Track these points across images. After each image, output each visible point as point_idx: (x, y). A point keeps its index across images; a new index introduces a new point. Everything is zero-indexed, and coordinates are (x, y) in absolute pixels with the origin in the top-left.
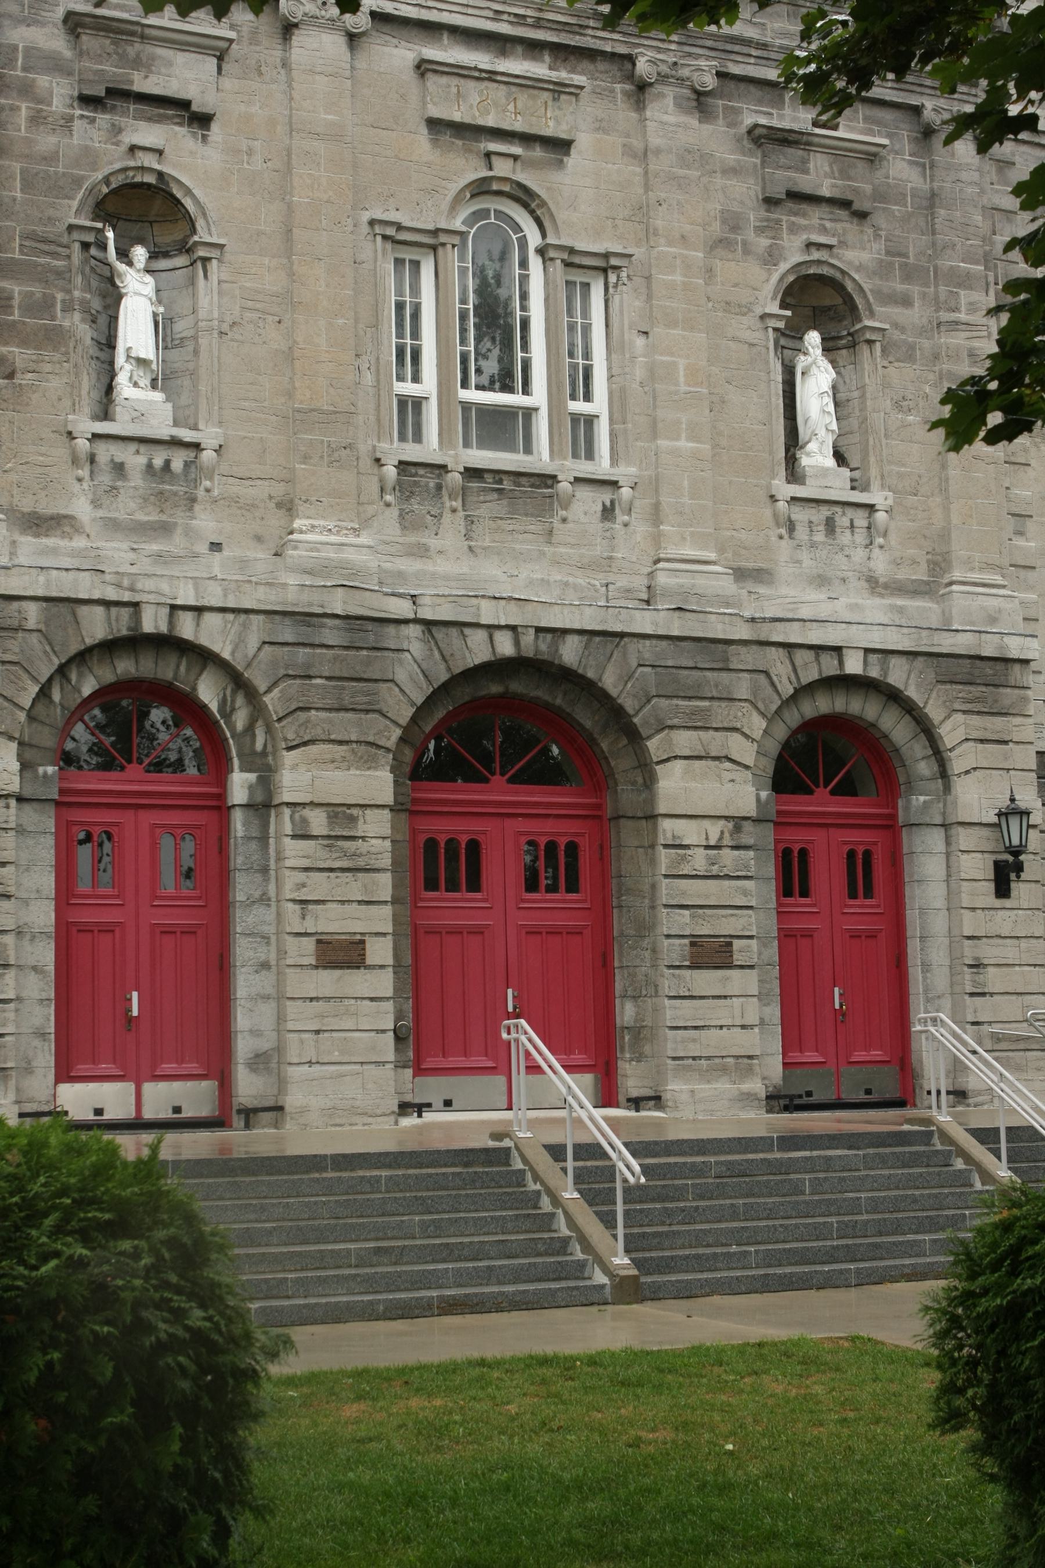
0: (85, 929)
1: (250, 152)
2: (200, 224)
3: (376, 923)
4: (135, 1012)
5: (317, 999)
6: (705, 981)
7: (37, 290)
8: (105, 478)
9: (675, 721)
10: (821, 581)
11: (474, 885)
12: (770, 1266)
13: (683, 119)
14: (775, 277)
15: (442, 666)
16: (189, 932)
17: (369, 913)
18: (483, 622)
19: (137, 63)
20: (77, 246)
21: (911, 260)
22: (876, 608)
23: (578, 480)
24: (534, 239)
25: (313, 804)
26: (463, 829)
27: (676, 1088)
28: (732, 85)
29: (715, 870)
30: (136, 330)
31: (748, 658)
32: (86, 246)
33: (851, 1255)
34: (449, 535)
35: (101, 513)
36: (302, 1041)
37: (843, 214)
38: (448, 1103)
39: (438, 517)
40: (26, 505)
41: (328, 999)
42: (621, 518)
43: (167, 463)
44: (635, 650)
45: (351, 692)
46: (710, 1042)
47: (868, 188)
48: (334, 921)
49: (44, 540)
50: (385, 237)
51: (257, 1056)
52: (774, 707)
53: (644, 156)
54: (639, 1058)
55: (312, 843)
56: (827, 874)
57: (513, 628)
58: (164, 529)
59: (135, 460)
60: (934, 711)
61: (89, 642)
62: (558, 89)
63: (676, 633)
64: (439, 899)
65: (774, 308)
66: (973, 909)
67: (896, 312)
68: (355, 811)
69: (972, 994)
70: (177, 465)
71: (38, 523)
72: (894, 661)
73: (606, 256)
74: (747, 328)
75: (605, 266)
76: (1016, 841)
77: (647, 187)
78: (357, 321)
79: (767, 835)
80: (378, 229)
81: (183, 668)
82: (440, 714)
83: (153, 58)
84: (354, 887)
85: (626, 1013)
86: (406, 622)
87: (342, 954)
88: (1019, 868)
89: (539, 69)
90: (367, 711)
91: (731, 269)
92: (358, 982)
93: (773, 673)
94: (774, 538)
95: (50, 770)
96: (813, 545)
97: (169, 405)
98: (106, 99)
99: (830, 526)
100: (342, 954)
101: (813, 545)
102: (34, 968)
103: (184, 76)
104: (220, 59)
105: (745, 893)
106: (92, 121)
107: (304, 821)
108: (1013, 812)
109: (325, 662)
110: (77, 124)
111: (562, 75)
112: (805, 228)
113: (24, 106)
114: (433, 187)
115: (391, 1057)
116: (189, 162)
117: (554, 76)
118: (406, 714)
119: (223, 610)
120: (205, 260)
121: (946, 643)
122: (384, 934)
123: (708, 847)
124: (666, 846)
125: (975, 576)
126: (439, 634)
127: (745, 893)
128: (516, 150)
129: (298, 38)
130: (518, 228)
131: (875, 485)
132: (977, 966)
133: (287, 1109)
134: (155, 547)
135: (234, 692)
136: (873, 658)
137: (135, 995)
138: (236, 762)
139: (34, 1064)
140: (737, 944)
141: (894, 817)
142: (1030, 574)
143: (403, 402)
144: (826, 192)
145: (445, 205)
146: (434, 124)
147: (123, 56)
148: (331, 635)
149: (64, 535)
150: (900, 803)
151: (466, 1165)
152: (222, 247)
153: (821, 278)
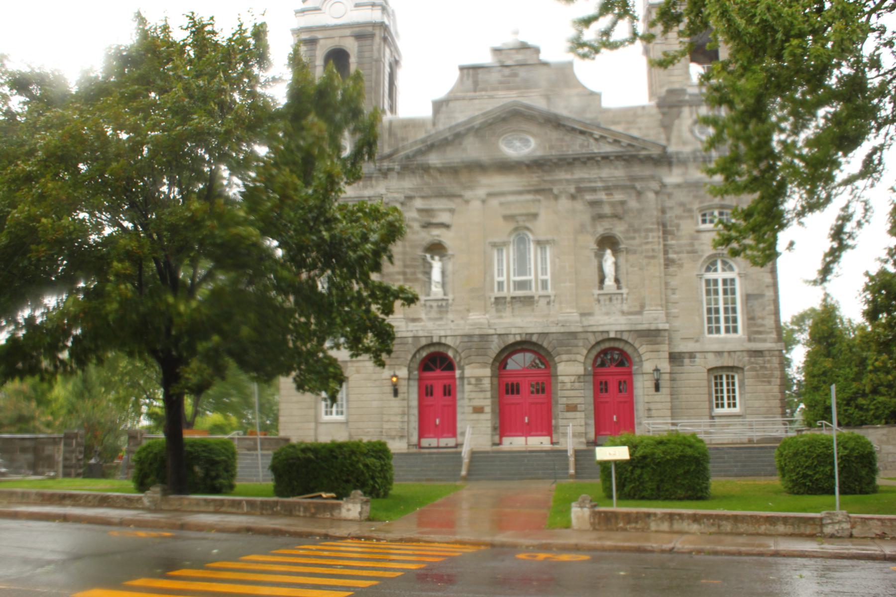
6: (570, 415)
7: (412, 270)
10: (608, 314)
11: (518, 392)
17: (486, 401)
19: (433, 217)
22: (623, 320)
23: (540, 297)
27: (562, 440)
30: (436, 275)
31: (582, 336)
40: (411, 316)
42: (552, 304)
44: (551, 337)
48: (477, 403)
54: (556, 433)
57: (520, 334)
58: (441, 319)
59: (434, 304)
60: (637, 345)
64: (507, 396)
67: (632, 242)
71: (414, 320)
75: (547, 242)
79: (590, 379)
84: (482, 395)
87: (478, 410)
96: (605, 305)
98: (427, 225)
99: (611, 300)
100: (478, 410)
102: (414, 415)
103: (444, 218)
104: (452, 211)
108: (657, 370)
118: (494, 355)
121: (639, 327)
132: (649, 410)
148: (476, 339)
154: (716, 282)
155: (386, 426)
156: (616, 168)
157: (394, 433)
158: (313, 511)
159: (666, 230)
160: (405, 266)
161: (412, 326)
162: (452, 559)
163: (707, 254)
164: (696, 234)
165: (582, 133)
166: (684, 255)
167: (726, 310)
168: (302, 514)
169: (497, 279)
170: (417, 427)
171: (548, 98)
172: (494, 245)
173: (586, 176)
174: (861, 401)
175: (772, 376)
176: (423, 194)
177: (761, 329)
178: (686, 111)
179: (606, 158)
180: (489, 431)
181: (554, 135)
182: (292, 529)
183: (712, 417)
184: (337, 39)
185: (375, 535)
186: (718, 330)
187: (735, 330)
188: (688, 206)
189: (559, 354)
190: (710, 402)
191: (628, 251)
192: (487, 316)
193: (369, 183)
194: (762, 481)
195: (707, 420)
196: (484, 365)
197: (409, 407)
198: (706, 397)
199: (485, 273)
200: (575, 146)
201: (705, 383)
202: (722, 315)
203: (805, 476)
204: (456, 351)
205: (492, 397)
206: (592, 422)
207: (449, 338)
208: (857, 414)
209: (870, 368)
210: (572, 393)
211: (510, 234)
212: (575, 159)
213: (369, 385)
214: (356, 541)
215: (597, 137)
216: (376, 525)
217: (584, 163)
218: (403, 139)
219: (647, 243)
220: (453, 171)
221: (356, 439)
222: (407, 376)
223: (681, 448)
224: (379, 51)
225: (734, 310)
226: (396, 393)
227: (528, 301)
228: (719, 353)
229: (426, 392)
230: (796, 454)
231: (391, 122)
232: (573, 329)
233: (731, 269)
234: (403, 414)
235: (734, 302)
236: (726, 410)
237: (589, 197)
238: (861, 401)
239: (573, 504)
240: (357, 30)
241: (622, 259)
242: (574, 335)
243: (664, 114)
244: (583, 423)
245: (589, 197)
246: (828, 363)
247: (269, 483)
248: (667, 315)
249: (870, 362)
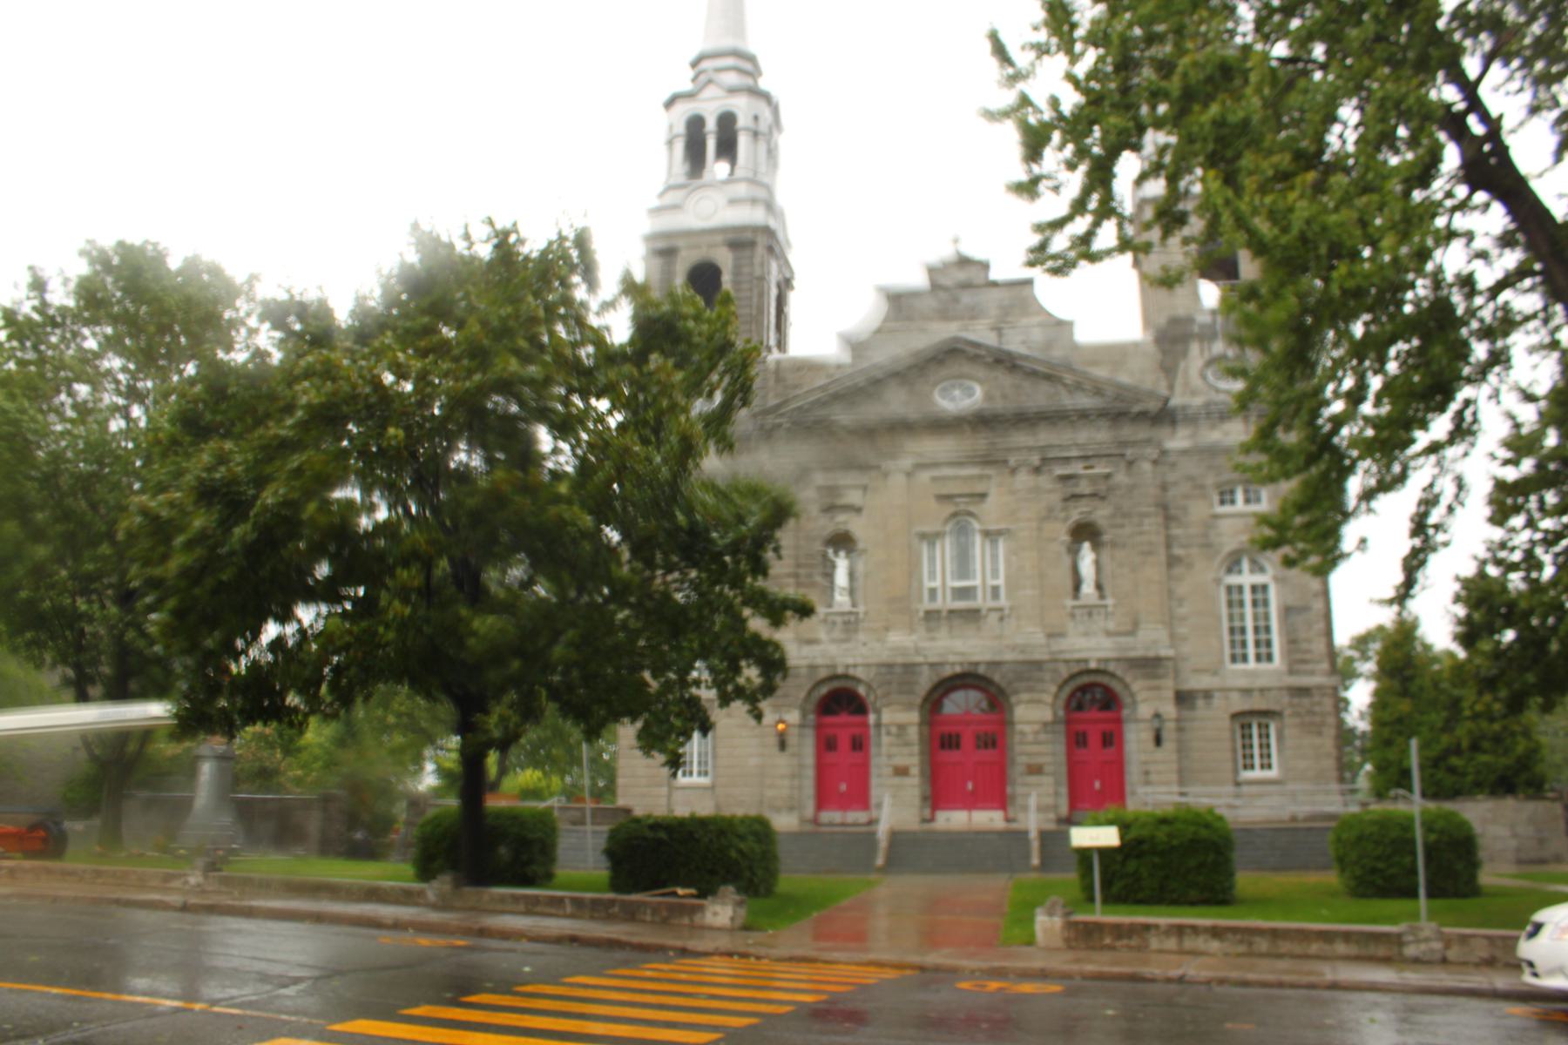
10: (1086, 634)
17: (912, 758)
23: (990, 610)
27: (1021, 816)
30: (841, 578)
34: (943, 632)
48: (900, 761)
56: (1094, 739)
59: (839, 619)
60: (1128, 679)
62: (981, 477)
71: (812, 642)
75: (1000, 533)
79: (1062, 728)
84: (906, 750)
87: (902, 772)
92: (907, 781)
98: (830, 509)
100: (902, 772)
103: (854, 497)
104: (865, 488)
108: (1157, 716)
121: (1132, 654)
132: (1147, 773)
154: (1240, 588)
155: (769, 793)
158: (665, 914)
159: (1168, 515)
160: (798, 566)
161: (807, 650)
162: (865, 988)
163: (1227, 549)
165: (1048, 377)
166: (1194, 551)
167: (1256, 630)
168: (648, 918)
169: (928, 584)
171: (998, 330)
172: (923, 536)
173: (1057, 442)
174: (1455, 761)
175: (1323, 724)
177: (1308, 657)
178: (1195, 348)
179: (1084, 415)
180: (917, 801)
181: (1006, 380)
182: (635, 940)
183: (1238, 784)
185: (752, 950)
186: (1245, 658)
187: (1269, 658)
189: (1016, 692)
190: (1235, 761)
191: (1114, 545)
192: (914, 637)
194: (1313, 878)
195: (1230, 789)
196: (908, 707)
197: (801, 766)
198: (1229, 755)
199: (910, 579)
200: (1038, 397)
201: (1227, 735)
202: (1250, 637)
203: (1374, 871)
204: (869, 687)
205: (922, 753)
206: (1064, 790)
208: (1449, 780)
209: (1467, 713)
210: (1035, 748)
211: (946, 521)
214: (727, 959)
216: (754, 937)
218: (796, 387)
219: (1141, 533)
221: (727, 812)
223: (1192, 829)
224: (762, 264)
225: (1268, 629)
226: (783, 745)
227: (973, 615)
228: (1247, 692)
229: (826, 745)
230: (1360, 838)
231: (778, 363)
232: (1037, 656)
233: (1262, 570)
234: (793, 776)
235: (1267, 617)
236: (1257, 774)
238: (1455, 761)
239: (1038, 910)
240: (731, 236)
241: (1106, 555)
242: (1038, 665)
243: (1164, 352)
244: (1051, 790)
245: (1060, 470)
246: (1405, 706)
247: (603, 873)
248: (1172, 636)
249: (1465, 704)
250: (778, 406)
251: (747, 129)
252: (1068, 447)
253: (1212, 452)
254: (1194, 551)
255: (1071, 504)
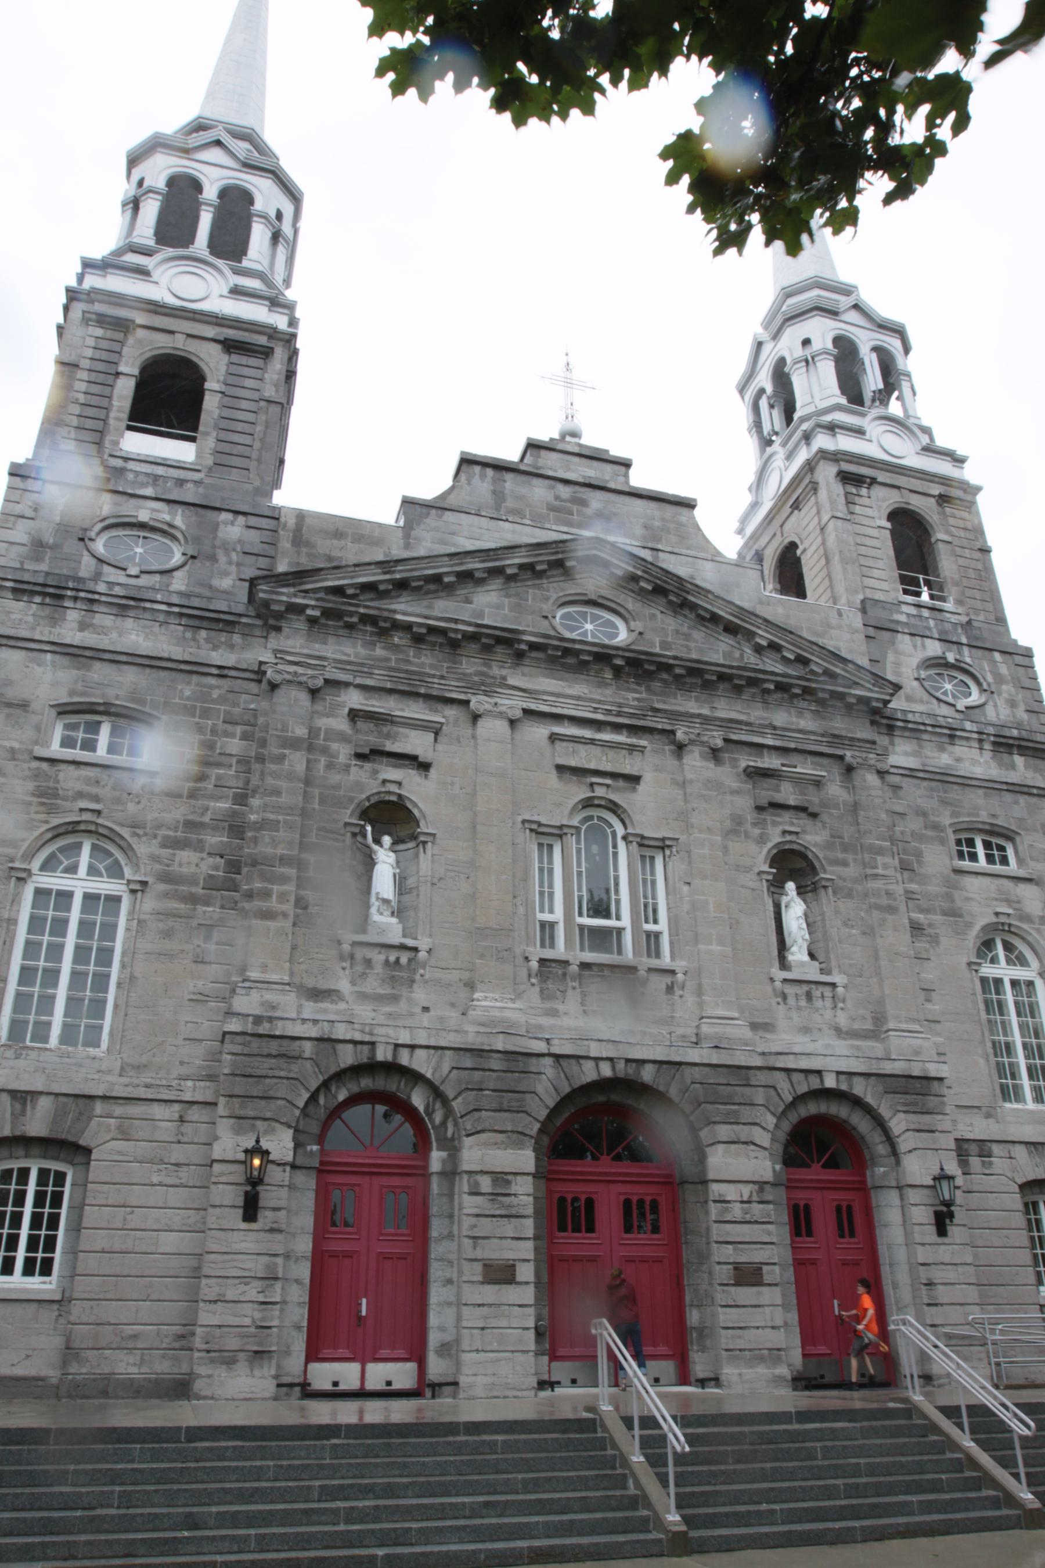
0: (334, 1255)
1: (453, 784)
2: (422, 823)
3: (524, 1254)
4: (364, 1313)
5: (482, 1305)
6: (745, 1294)
8: (359, 968)
9: (717, 1119)
10: (806, 1030)
11: (591, 1229)
12: (792, 1522)
13: (705, 764)
14: (765, 851)
15: (566, 1084)
16: (402, 1258)
18: (592, 1055)
19: (388, 736)
20: (349, 835)
21: (846, 840)
22: (842, 1047)
23: (651, 970)
24: (620, 831)
25: (483, 1172)
26: (583, 1190)
27: (729, 1372)
28: (732, 746)
29: (748, 1217)
31: (762, 1078)
32: (354, 835)
33: (856, 1513)
34: (571, 1004)
35: (356, 989)
36: (472, 1335)
37: (803, 815)
38: (574, 1381)
39: (564, 992)
40: (310, 983)
41: (490, 1305)
43: (398, 959)
44: (689, 1073)
45: (508, 1099)
46: (749, 1339)
47: (816, 800)
49: (320, 1005)
50: (531, 830)
51: (443, 1345)
52: (781, 1109)
53: (683, 784)
54: (703, 1349)
55: (481, 1198)
56: (824, 1221)
57: (611, 1059)
58: (394, 998)
59: (378, 957)
60: (885, 1112)
61: (342, 1066)
63: (715, 1062)
65: (766, 868)
66: (923, 1244)
67: (840, 869)
68: (509, 1177)
69: (929, 1305)
70: (404, 960)
71: (317, 994)
72: (856, 1080)
73: (663, 839)
74: (749, 880)
75: (663, 846)
76: (947, 1197)
77: (686, 800)
78: (514, 877)
79: (781, 1194)
80: (527, 825)
81: (402, 1084)
82: (566, 1115)
83: (397, 733)
84: (508, 1228)
85: (693, 1317)
86: (543, 1055)
88: (951, 1215)
89: (621, 738)
90: (518, 1112)
91: (737, 846)
93: (778, 1087)
94: (774, 1004)
95: (315, 1148)
96: (799, 1008)
97: (400, 926)
99: (809, 996)
100: (501, 1274)
101: (799, 1008)
102: (297, 1281)
103: (416, 743)
104: (436, 734)
105: (769, 1233)
106: (362, 767)
107: (477, 1183)
109: (491, 1081)
110: (353, 769)
111: (633, 741)
112: (781, 823)
113: (323, 759)
114: (560, 802)
115: (532, 1346)
116: (416, 789)
117: (629, 741)
119: (428, 1047)
120: (424, 843)
121: (888, 1068)
122: (528, 1261)
123: (742, 1202)
124: (715, 1201)
125: (904, 1026)
126: (564, 1063)
127: (769, 1233)
128: (608, 781)
129: (481, 723)
130: (610, 826)
131: (835, 971)
132: (930, 1284)
133: (461, 1384)
134: (388, 1009)
135: (435, 1099)
136: (842, 1077)
137: (364, 1301)
138: (434, 1144)
139: (292, 1348)
140: (765, 1268)
141: (864, 1182)
142: (938, 1026)
143: (543, 924)
144: (792, 803)
145: (567, 811)
146: (560, 768)
147: (380, 732)
148: (495, 1063)
149: (332, 1002)
150: (868, 1173)
151: (564, 1432)
152: (434, 835)
153: (792, 852)
154: (998, 982)
156: (800, 715)
157: (233, 1343)
161: (310, 1010)
164: (953, 876)
165: (731, 629)
170: (305, 1323)
172: (537, 830)
176: (369, 682)
179: (782, 687)
184: (180, 337)
188: (932, 818)
193: (223, 637)
200: (717, 651)
207: (420, 1053)
212: (722, 677)
213: (155, 1179)
215: (764, 643)
217: (738, 690)
218: (330, 559)
219: (876, 876)
220: (449, 641)
222: (290, 1158)
232: (741, 1059)
233: (1022, 961)
237: (746, 760)
250: (298, 576)
251: (264, 217)
252: (759, 729)
253: (944, 779)
254: (937, 918)
255: (768, 817)
